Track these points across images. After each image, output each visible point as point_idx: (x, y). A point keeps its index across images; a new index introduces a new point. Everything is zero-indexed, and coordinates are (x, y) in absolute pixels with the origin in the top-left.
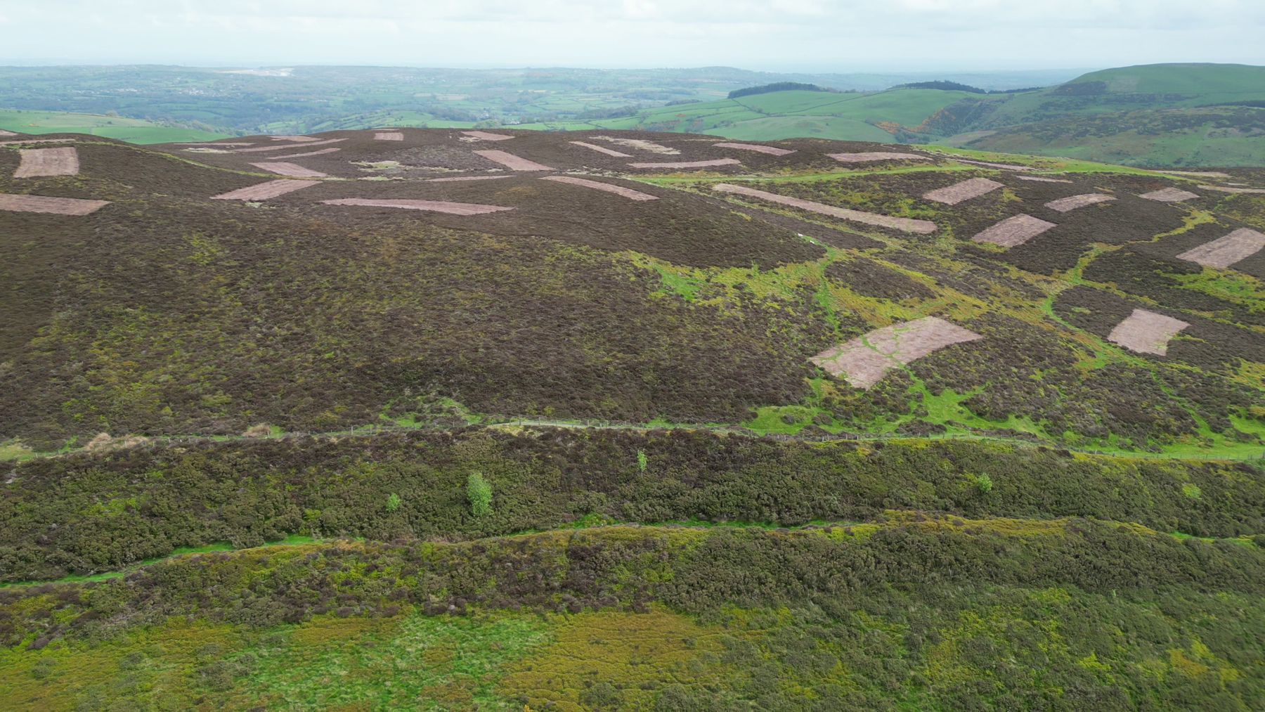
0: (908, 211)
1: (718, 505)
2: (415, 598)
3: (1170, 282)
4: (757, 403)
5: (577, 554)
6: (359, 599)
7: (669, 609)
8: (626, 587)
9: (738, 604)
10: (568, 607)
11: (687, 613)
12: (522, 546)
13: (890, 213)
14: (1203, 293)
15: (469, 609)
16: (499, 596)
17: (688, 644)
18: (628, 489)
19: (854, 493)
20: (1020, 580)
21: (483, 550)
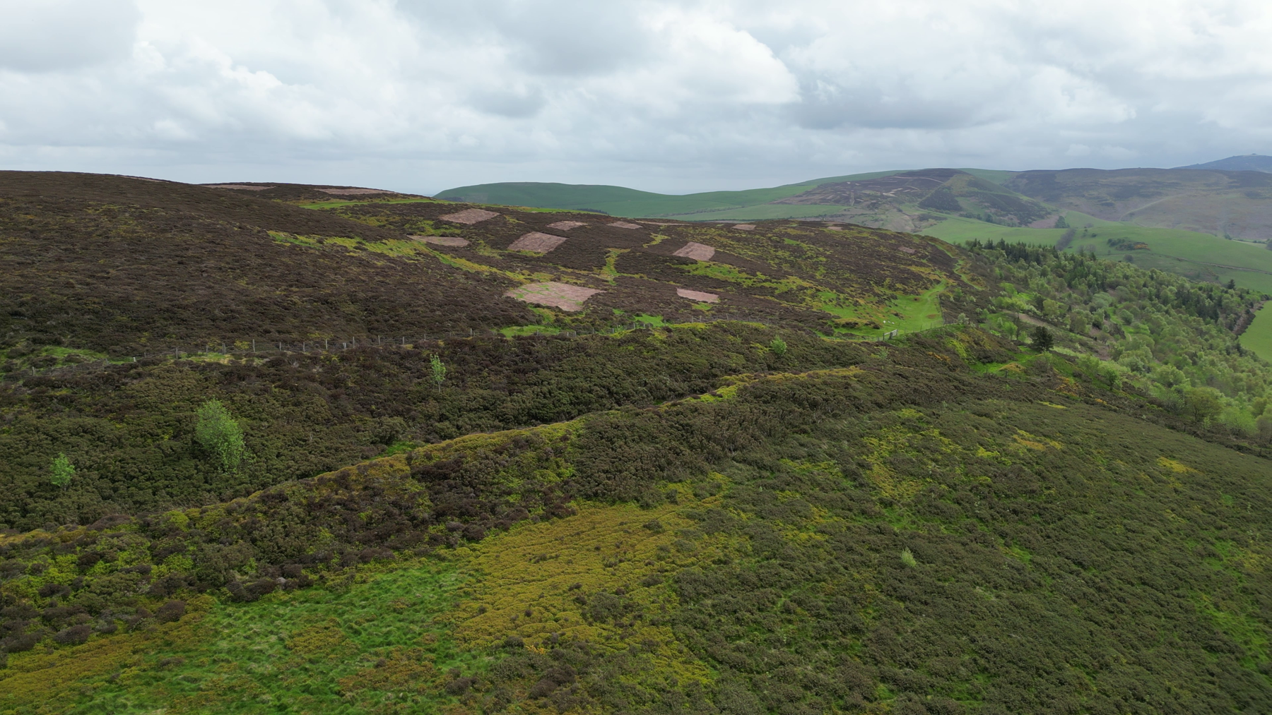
0: (433, 231)
1: (552, 406)
2: (205, 582)
3: (682, 271)
4: (496, 324)
5: (432, 476)
6: (93, 611)
7: (597, 503)
8: (526, 494)
9: (671, 480)
10: (463, 536)
11: (623, 501)
12: (343, 481)
13: (416, 233)
14: (707, 277)
15: (312, 577)
16: (348, 549)
17: (654, 528)
18: (432, 407)
19: (681, 372)
20: (880, 406)
21: (282, 498)
